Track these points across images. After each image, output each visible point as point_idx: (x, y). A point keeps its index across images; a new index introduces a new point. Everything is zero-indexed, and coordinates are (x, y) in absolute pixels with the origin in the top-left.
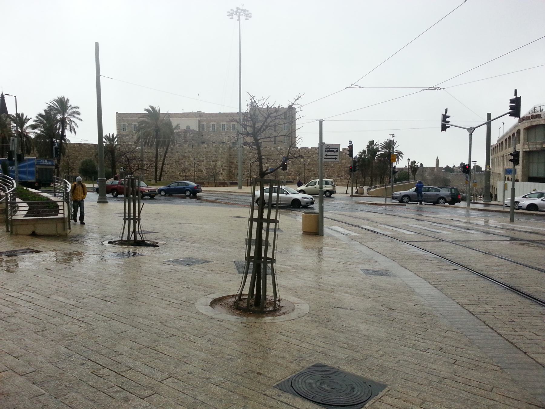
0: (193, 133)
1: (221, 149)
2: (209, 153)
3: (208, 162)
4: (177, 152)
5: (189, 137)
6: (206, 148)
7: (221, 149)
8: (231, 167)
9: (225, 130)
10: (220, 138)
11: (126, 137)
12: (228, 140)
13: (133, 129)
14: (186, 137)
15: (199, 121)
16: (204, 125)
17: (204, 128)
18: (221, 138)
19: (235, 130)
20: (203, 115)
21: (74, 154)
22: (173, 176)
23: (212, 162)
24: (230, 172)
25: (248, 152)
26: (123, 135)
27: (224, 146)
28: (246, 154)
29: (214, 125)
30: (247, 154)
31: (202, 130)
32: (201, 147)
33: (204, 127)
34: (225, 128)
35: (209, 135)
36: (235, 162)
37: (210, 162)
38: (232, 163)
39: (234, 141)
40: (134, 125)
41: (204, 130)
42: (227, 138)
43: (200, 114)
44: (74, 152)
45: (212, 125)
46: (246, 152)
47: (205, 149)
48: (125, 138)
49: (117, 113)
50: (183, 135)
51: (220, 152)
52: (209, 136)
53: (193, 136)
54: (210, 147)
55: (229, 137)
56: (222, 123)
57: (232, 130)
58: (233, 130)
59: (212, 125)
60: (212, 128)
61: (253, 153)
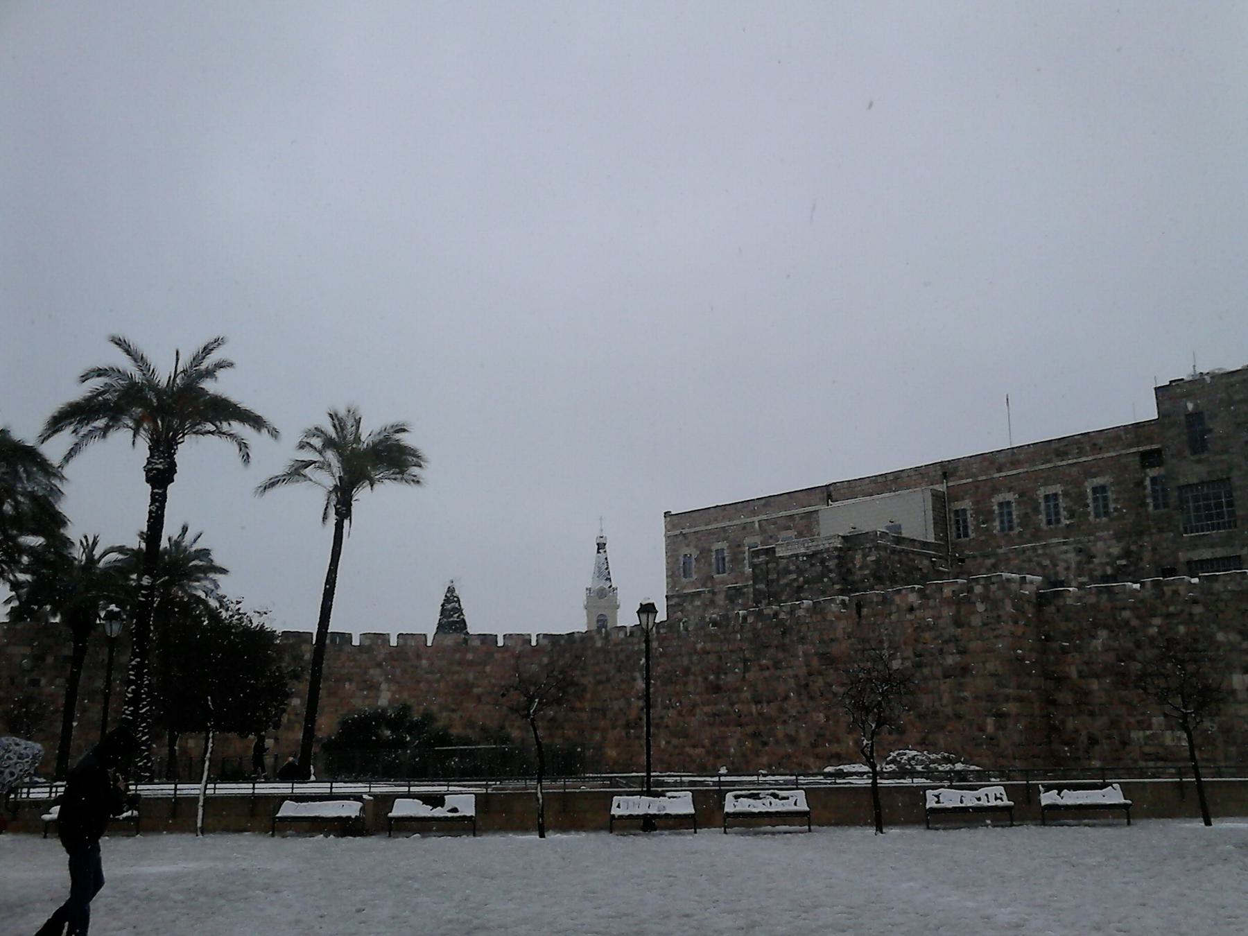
0: (878, 547)
1: (980, 607)
2: (927, 635)
3: (925, 679)
4: (802, 640)
5: (860, 568)
6: (911, 609)
7: (980, 607)
8: (1054, 703)
9: (1058, 521)
10: (1039, 564)
11: (692, 601)
12: (1079, 563)
13: (714, 567)
14: (849, 571)
15: (937, 496)
16: (964, 510)
17: (966, 528)
18: (1047, 562)
19: (1106, 514)
20: (956, 469)
21: (456, 677)
22: (789, 756)
23: (946, 677)
24: (1055, 729)
25: (1134, 609)
26: (687, 595)
27: (994, 587)
28: (1127, 623)
29: (1009, 503)
30: (1135, 623)
31: (959, 536)
32: (894, 609)
33: (965, 521)
34: (1057, 513)
35: (986, 556)
36: (1074, 675)
37: (935, 678)
38: (1061, 680)
39: (1109, 571)
40: (717, 551)
41: (966, 535)
42: (1072, 557)
43: (946, 470)
44: (458, 668)
45: (1001, 505)
46: (1126, 614)
47: (909, 617)
48: (690, 608)
49: (667, 514)
50: (836, 561)
51: (976, 621)
52: (992, 561)
53: (877, 562)
54: (931, 603)
55: (1080, 551)
56: (1042, 492)
57: (1091, 518)
58: (1097, 516)
59: (1001, 505)
60: (1002, 522)
61: (1169, 616)
